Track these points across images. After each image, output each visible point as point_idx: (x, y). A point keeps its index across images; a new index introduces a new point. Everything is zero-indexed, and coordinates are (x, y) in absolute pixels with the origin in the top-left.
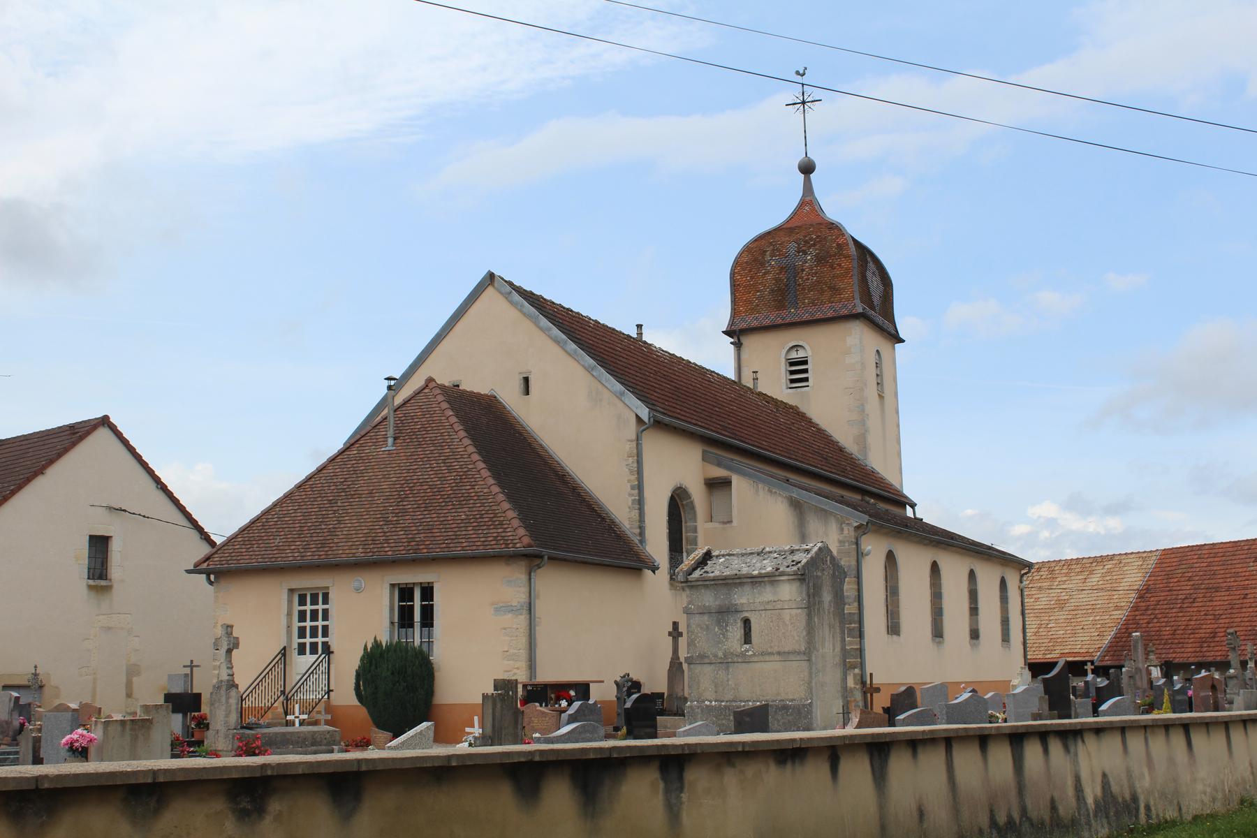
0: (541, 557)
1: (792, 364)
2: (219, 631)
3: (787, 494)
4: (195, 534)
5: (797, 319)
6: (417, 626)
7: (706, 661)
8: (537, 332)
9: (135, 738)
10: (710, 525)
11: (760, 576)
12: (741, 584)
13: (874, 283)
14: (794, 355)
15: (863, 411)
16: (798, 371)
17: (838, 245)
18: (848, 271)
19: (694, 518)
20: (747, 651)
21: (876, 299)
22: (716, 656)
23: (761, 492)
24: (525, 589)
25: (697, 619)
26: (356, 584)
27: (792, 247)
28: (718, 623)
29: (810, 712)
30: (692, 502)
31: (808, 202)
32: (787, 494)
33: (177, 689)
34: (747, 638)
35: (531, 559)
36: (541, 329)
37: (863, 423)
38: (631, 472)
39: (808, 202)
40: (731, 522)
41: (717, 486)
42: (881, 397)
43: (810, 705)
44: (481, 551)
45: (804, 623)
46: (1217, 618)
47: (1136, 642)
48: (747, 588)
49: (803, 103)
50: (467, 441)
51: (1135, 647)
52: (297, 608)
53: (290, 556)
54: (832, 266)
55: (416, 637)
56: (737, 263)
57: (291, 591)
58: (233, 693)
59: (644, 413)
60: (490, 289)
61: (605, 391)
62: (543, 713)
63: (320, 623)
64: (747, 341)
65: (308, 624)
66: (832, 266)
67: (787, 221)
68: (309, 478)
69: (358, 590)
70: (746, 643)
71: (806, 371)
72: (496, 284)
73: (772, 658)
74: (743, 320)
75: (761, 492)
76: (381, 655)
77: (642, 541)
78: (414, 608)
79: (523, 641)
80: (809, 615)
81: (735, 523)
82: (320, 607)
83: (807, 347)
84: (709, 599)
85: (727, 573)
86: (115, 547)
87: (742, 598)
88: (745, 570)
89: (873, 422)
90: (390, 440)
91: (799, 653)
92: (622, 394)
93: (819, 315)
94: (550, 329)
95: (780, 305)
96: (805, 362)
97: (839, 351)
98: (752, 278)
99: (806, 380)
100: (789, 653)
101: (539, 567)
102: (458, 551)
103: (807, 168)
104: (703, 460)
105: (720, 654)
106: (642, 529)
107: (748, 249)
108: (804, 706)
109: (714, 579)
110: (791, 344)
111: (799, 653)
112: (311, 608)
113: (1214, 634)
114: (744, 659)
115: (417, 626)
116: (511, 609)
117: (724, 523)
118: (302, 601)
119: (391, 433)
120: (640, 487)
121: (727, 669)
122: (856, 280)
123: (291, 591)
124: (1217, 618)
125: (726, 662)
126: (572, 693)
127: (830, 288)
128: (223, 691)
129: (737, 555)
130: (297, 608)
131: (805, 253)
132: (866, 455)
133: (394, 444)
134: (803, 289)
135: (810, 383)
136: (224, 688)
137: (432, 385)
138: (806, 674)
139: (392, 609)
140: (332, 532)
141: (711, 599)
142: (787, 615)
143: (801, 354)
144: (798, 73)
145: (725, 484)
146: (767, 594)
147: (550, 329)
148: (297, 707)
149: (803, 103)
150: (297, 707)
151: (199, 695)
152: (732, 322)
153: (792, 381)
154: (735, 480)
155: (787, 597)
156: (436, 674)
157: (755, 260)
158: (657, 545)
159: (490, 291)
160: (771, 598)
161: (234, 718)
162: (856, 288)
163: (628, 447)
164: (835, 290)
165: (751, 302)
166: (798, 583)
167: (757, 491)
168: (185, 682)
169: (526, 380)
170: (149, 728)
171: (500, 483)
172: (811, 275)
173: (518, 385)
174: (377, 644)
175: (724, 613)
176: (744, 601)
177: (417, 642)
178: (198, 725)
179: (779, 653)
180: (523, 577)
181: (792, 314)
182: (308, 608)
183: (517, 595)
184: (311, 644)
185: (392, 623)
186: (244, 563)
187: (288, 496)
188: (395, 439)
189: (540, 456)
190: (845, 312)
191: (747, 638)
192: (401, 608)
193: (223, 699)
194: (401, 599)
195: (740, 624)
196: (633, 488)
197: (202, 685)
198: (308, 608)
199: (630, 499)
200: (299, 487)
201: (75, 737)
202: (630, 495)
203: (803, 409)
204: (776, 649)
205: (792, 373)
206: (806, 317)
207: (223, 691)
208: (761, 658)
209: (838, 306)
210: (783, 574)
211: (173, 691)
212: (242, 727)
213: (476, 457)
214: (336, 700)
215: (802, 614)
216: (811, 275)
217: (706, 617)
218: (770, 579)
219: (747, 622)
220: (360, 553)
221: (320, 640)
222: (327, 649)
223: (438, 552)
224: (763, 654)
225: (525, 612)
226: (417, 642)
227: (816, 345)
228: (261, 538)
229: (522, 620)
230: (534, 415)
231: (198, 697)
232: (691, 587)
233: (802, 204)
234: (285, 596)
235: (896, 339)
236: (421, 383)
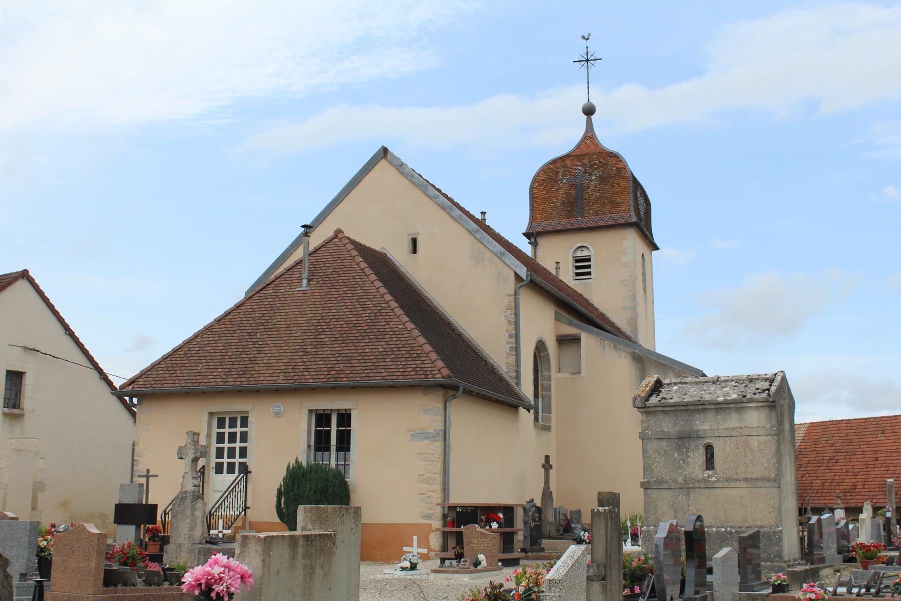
0: (455, 388)
1: (577, 261)
2: (183, 440)
3: (631, 350)
4: (95, 374)
5: (583, 225)
6: (333, 449)
7: (665, 486)
8: (426, 199)
9: (310, 572)
11: (726, 402)
12: (704, 410)
13: (641, 201)
14: (579, 254)
15: (635, 299)
16: (583, 266)
17: (617, 168)
18: (625, 188)
19: (549, 369)
20: (710, 476)
21: (642, 213)
22: (675, 481)
23: (607, 348)
24: (441, 418)
25: (654, 444)
26: (276, 409)
27: (580, 169)
28: (678, 448)
29: (780, 540)
30: (548, 355)
31: (589, 136)
32: (631, 350)
33: (130, 499)
34: (710, 463)
35: (448, 390)
36: (429, 197)
37: (634, 309)
38: (509, 323)
39: (589, 136)
41: (567, 342)
42: (645, 290)
43: (781, 532)
44: (401, 380)
45: (773, 449)
46: (856, 474)
47: (891, 486)
48: (710, 415)
49: (587, 61)
50: (378, 284)
51: (890, 491)
52: (216, 430)
53: (213, 381)
54: (612, 185)
55: (332, 459)
56: (535, 180)
57: (211, 414)
58: (199, 504)
59: (523, 271)
60: (383, 162)
62: (483, 534)
63: (238, 445)
64: (543, 242)
65: (226, 445)
66: (612, 185)
67: (574, 151)
68: (228, 314)
69: (277, 415)
70: (707, 469)
71: (589, 267)
72: (389, 158)
73: (738, 484)
74: (539, 225)
75: (607, 348)
76: (304, 475)
78: (331, 432)
79: (439, 465)
80: (778, 442)
81: (583, 374)
82: (238, 430)
83: (590, 248)
84: (667, 425)
85: (687, 399)
86: (28, 381)
87: (704, 424)
88: (707, 397)
89: (640, 309)
90: (305, 282)
91: (768, 480)
92: (503, 254)
93: (601, 223)
94: (437, 197)
95: (570, 214)
96: (589, 260)
97: (612, 250)
98: (547, 193)
99: (589, 273)
100: (757, 479)
101: (454, 397)
102: (378, 380)
103: (589, 111)
104: (556, 319)
105: (680, 479)
106: (518, 372)
107: (544, 170)
108: (775, 533)
109: (675, 405)
110: (578, 245)
111: (768, 480)
112: (232, 430)
113: (855, 486)
114: (707, 485)
115: (333, 449)
116: (426, 436)
117: (575, 374)
118: (221, 424)
119: (305, 274)
120: (517, 336)
121: (688, 494)
122: (631, 195)
123: (211, 414)
124: (856, 474)
125: (687, 487)
126: (501, 515)
127: (610, 202)
128: (188, 503)
129: (691, 383)
130: (216, 430)
131: (590, 174)
133: (308, 285)
134: (589, 202)
136: (189, 499)
137: (340, 236)
138: (777, 500)
139: (309, 434)
140: (253, 361)
141: (670, 425)
142: (754, 442)
143: (585, 253)
144: (583, 37)
145: (575, 340)
146: (732, 421)
147: (437, 197)
148: (221, 521)
149: (587, 61)
150: (221, 521)
151: (154, 507)
152: (530, 226)
153: (577, 274)
154: (584, 337)
155: (755, 424)
156: (352, 495)
157: (550, 178)
158: (527, 389)
159: (383, 164)
160: (738, 425)
161: (199, 531)
162: (631, 203)
163: (506, 300)
165: (546, 211)
166: (767, 410)
167: (603, 347)
168: (140, 493)
169: (414, 241)
170: (330, 554)
171: (412, 321)
172: (591, 192)
173: (407, 245)
174: (298, 465)
175: (684, 439)
176: (706, 427)
177: (333, 464)
178: (152, 538)
179: (746, 480)
180: (440, 406)
181: (579, 221)
182: (227, 430)
183: (434, 423)
184: (228, 464)
185: (309, 446)
186: (168, 386)
187: (209, 328)
188: (309, 280)
189: (429, 306)
190: (622, 221)
191: (710, 463)
192: (318, 433)
193: (188, 511)
194: (318, 424)
195: (702, 450)
196: (510, 336)
197: (161, 496)
198: (227, 430)
199: (508, 346)
200: (219, 320)
201: (217, 570)
202: (508, 343)
204: (742, 476)
205: (577, 268)
206: (591, 224)
207: (188, 503)
208: (726, 484)
209: (616, 216)
210: (751, 401)
211: (125, 501)
212: (207, 542)
213: (388, 297)
214: (253, 515)
215: (772, 441)
216: (591, 192)
217: (664, 443)
218: (738, 405)
219: (709, 449)
220: (281, 380)
221: (237, 460)
222: (245, 469)
223: (358, 381)
224: (727, 480)
225: (441, 439)
226: (333, 464)
227: (597, 246)
228: (183, 365)
229: (439, 444)
230: (420, 272)
231: (153, 509)
232: (648, 413)
233: (585, 138)
234: (205, 418)
235: (656, 248)
236: (331, 234)
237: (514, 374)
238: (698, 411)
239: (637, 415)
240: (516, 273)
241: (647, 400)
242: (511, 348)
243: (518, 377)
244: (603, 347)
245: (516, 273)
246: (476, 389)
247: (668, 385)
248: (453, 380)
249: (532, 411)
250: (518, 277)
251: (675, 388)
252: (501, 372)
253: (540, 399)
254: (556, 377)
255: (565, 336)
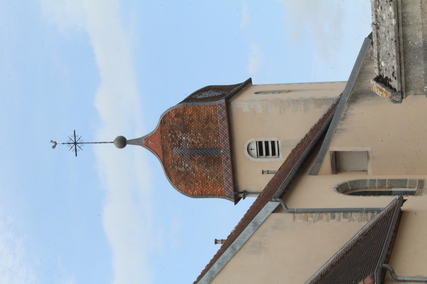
0: (384, 271)
1: (261, 154)
3: (346, 105)
5: (228, 148)
10: (370, 170)
11: (397, 16)
12: (404, 37)
13: (206, 95)
14: (255, 152)
15: (297, 101)
16: (266, 149)
17: (176, 116)
18: (194, 109)
19: (364, 181)
21: (217, 94)
27: (176, 151)
30: (350, 182)
31: (146, 142)
32: (346, 105)
37: (306, 101)
38: (320, 218)
39: (146, 142)
40: (367, 153)
41: (338, 164)
42: (289, 91)
48: (409, 31)
49: (75, 143)
54: (191, 121)
56: (185, 192)
59: (272, 205)
61: (253, 239)
64: (243, 186)
66: (191, 121)
71: (267, 143)
74: (227, 189)
77: (379, 211)
81: (368, 149)
83: (249, 141)
84: (418, 71)
85: (394, 52)
88: (392, 34)
89: (307, 95)
92: (255, 224)
93: (226, 132)
95: (217, 160)
96: (260, 143)
97: (251, 122)
98: (197, 181)
99: (273, 143)
101: (393, 272)
103: (122, 142)
104: (317, 174)
106: (367, 211)
107: (176, 184)
120: (333, 212)
122: (201, 104)
127: (207, 123)
129: (378, 49)
131: (181, 141)
132: (330, 99)
135: (275, 139)
141: (419, 68)
143: (254, 146)
144: (54, 147)
145: (336, 156)
149: (75, 143)
153: (274, 154)
157: (184, 178)
158: (384, 202)
162: (207, 104)
164: (209, 119)
165: (215, 183)
167: (343, 130)
176: (420, 35)
181: (224, 152)
190: (224, 113)
196: (333, 217)
199: (343, 220)
202: (339, 220)
203: (294, 146)
205: (267, 154)
206: (227, 141)
209: (220, 118)
216: (197, 141)
227: (247, 135)
233: (147, 146)
235: (249, 82)
237: (369, 214)
238: (405, 43)
239: (409, 99)
240: (273, 212)
241: (395, 90)
242: (345, 217)
243: (372, 211)
244: (343, 130)
245: (273, 212)
246: (384, 251)
247: (380, 70)
248: (377, 274)
249: (405, 198)
250: (277, 210)
251: (383, 64)
252: (367, 226)
253: (393, 190)
254: (372, 174)
255: (332, 166)
